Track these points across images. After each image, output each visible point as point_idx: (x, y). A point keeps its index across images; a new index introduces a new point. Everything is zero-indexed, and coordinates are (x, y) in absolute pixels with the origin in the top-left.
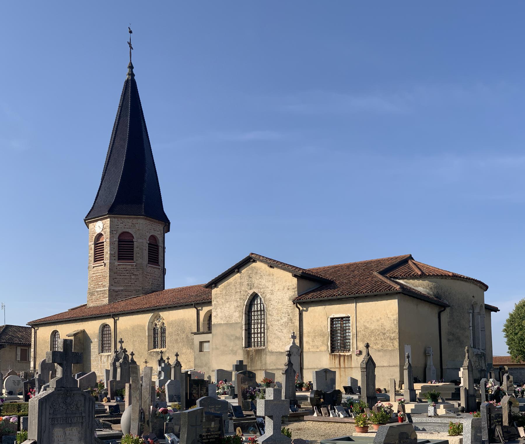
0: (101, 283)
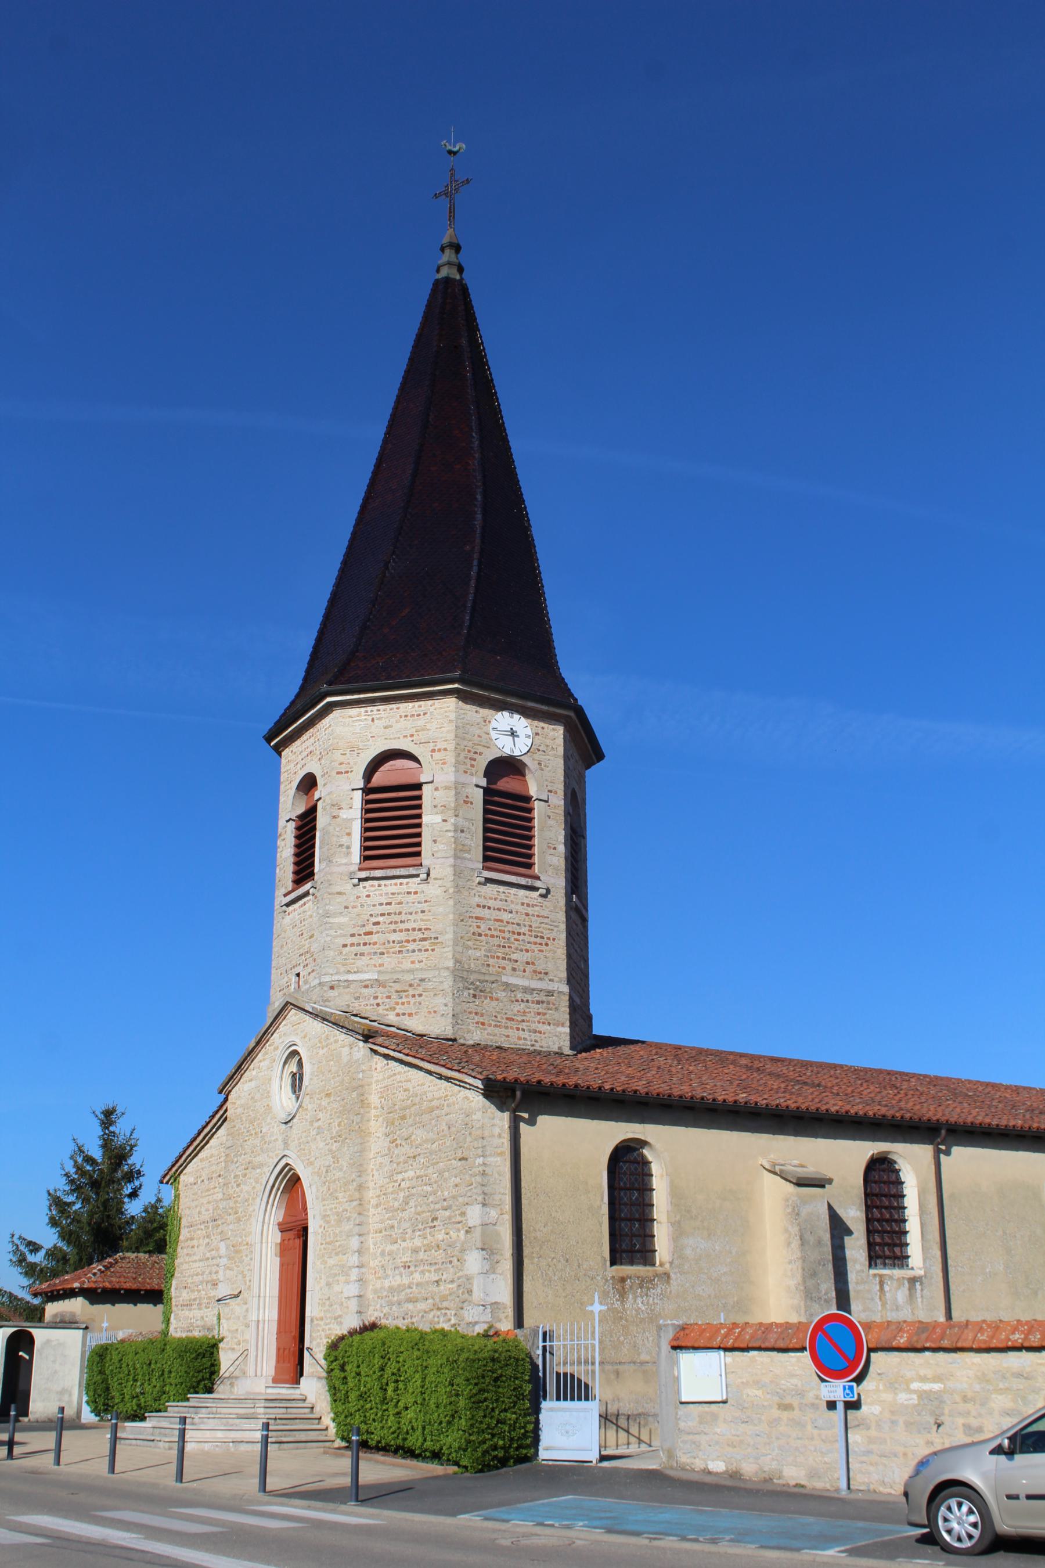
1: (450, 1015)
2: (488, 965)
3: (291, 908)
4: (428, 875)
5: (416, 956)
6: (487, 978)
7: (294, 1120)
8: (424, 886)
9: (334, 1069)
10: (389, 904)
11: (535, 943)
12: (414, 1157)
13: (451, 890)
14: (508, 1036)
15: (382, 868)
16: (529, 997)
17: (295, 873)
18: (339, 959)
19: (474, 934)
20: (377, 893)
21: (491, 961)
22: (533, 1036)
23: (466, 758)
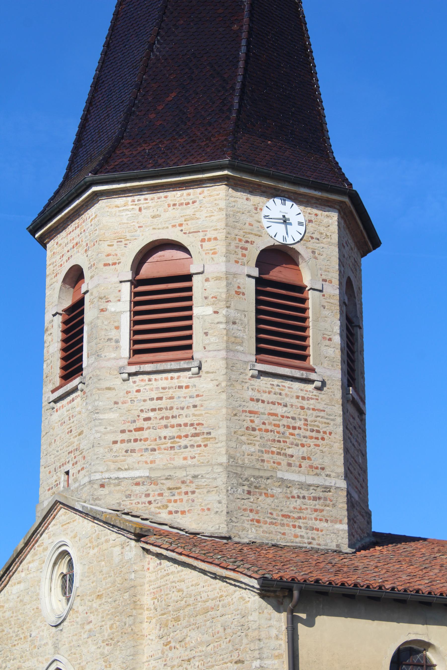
0: (303, 451)
1: (225, 513)
2: (263, 461)
3: (59, 404)
4: (200, 368)
5: (189, 452)
6: (261, 473)
7: (65, 623)
8: (195, 380)
9: (105, 570)
10: (160, 399)
11: (311, 438)
12: (189, 660)
13: (224, 384)
14: (284, 534)
15: (152, 362)
16: (304, 493)
17: (63, 368)
18: (108, 455)
19: (247, 428)
20: (147, 387)
21: (266, 457)
22: (311, 534)
23: (237, 247)
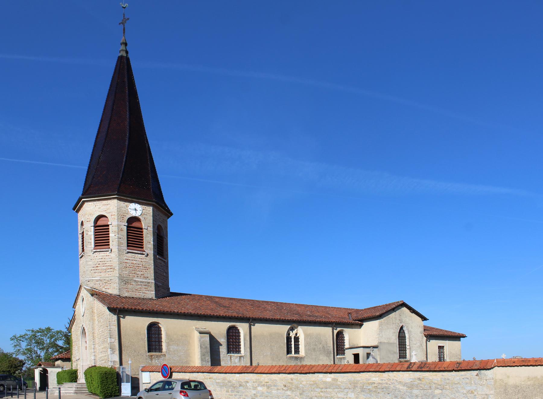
8: (110, 254)
